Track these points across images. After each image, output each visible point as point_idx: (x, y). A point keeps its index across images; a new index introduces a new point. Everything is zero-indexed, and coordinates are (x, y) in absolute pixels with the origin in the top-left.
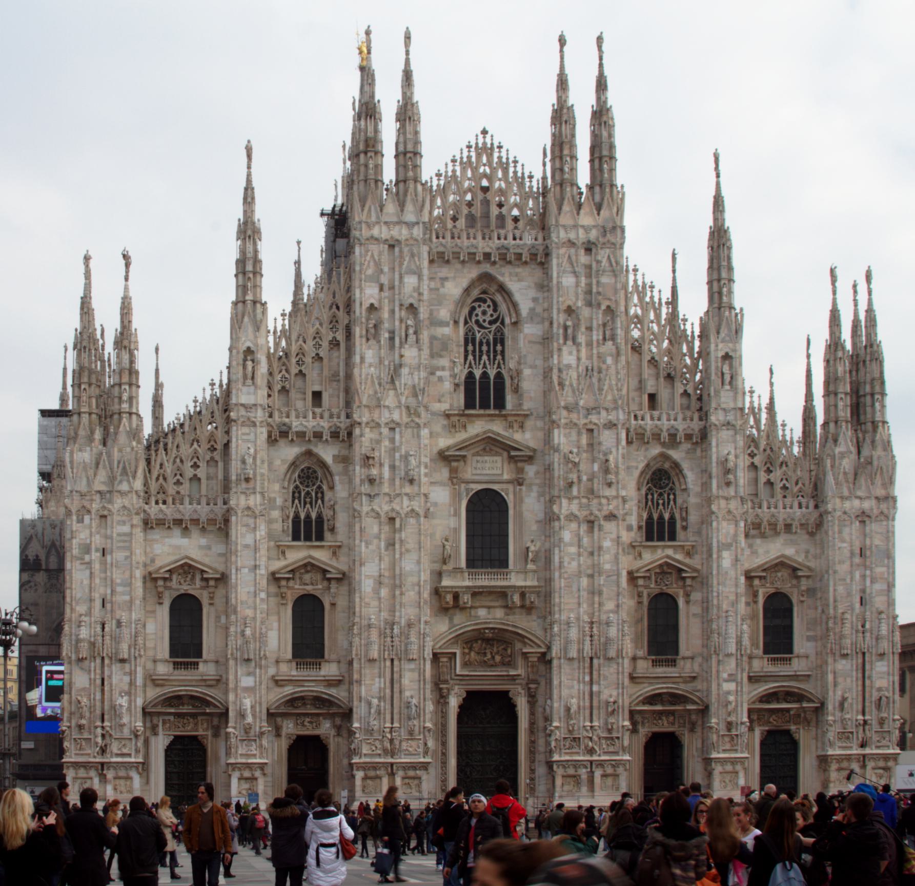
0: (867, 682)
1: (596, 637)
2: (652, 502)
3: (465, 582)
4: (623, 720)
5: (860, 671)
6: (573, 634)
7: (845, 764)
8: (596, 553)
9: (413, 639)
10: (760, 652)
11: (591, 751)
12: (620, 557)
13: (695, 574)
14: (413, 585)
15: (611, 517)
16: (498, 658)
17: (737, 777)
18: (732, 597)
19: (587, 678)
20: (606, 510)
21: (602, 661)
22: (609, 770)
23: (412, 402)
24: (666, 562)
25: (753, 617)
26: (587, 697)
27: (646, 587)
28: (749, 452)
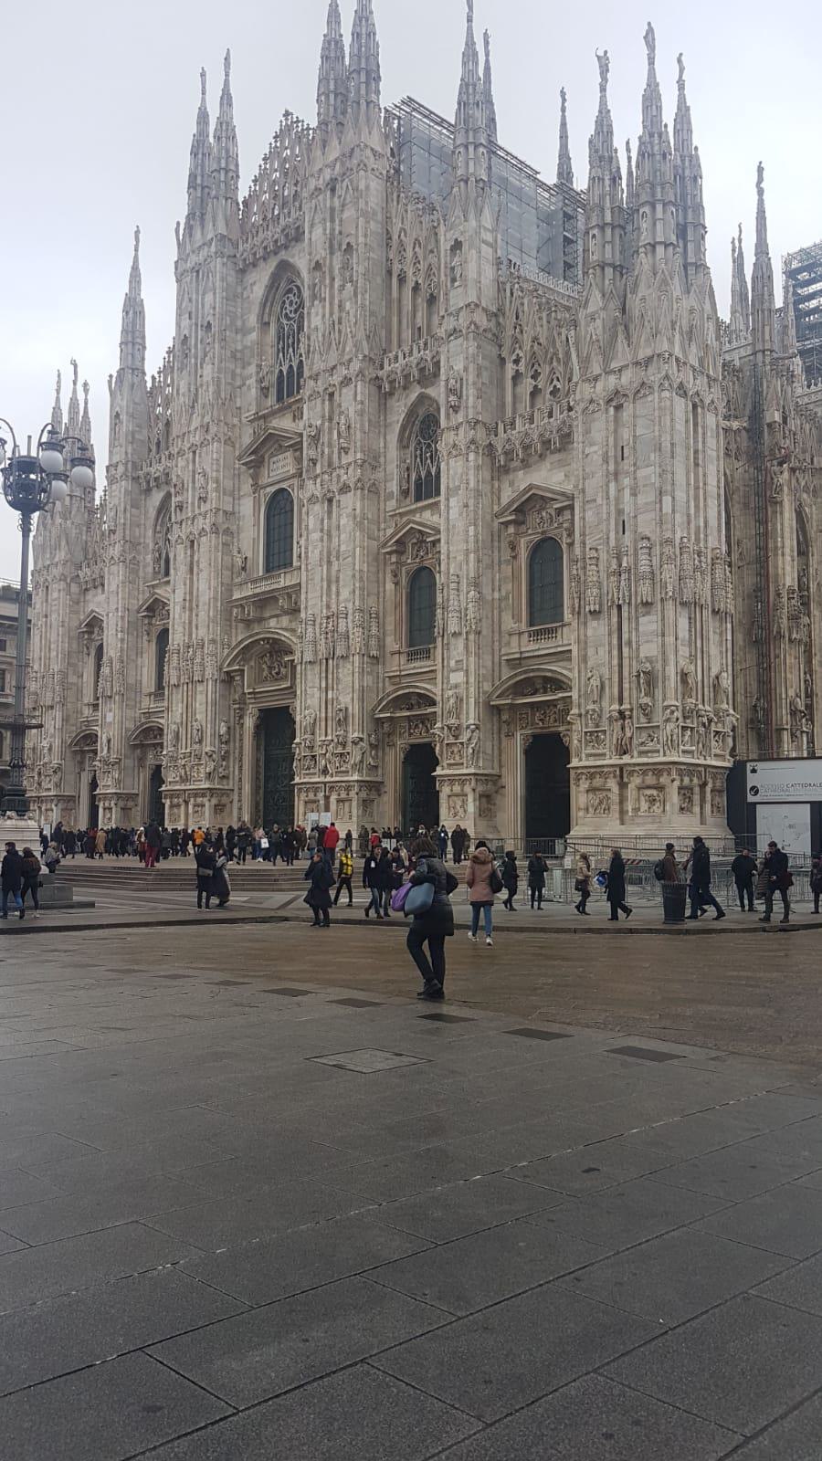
0: (625, 650)
3: (248, 591)
4: (354, 732)
5: (615, 636)
7: (598, 782)
9: (198, 660)
10: (524, 627)
11: (325, 772)
15: (345, 489)
17: (464, 803)
18: (461, 558)
19: (323, 685)
22: (343, 795)
23: (207, 419)
25: (515, 577)
28: (514, 357)
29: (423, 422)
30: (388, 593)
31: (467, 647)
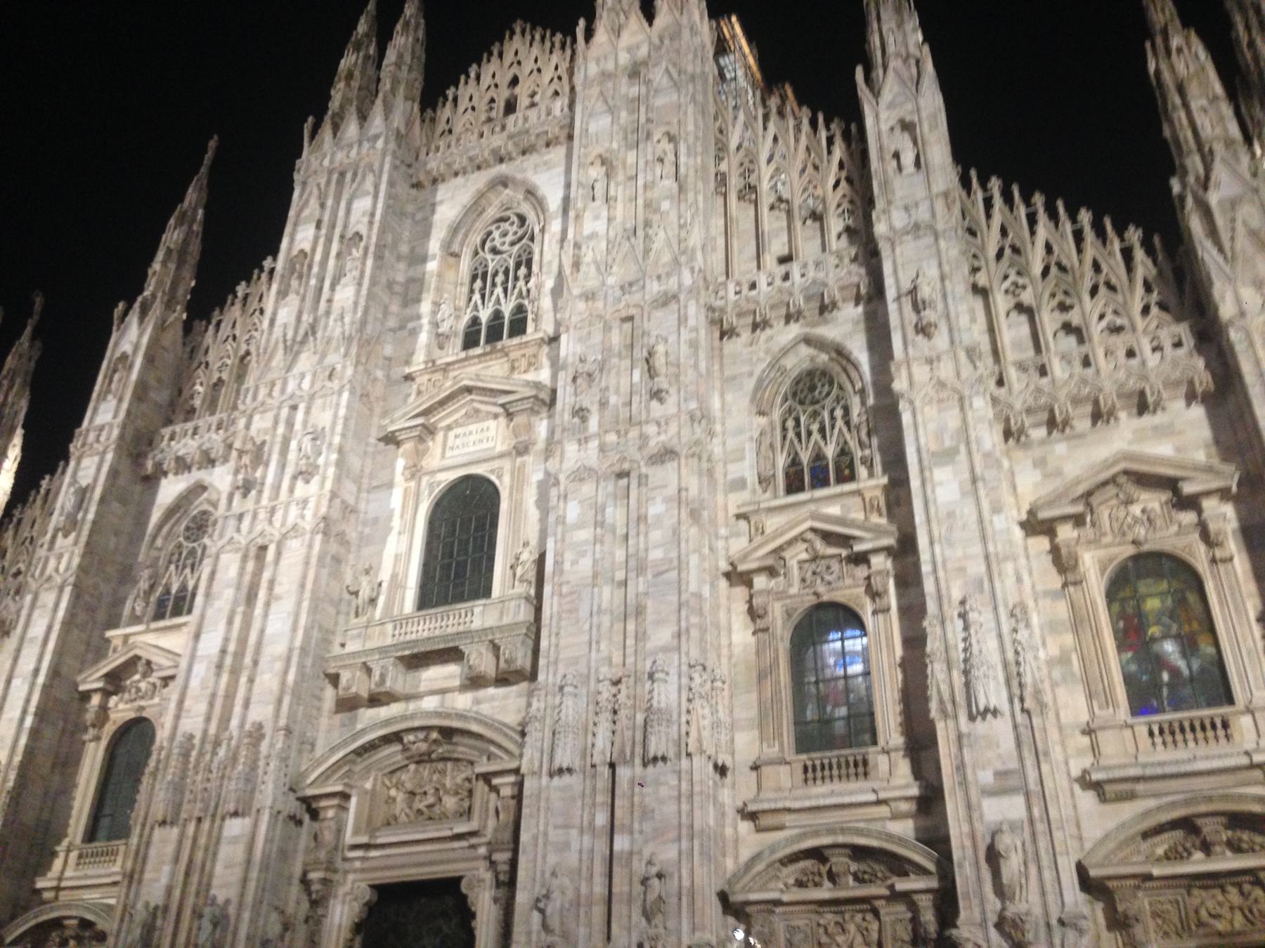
1: (623, 713)
2: (798, 435)
6: (572, 709)
8: (632, 533)
10: (1123, 712)
12: (683, 528)
13: (890, 541)
14: (274, 659)
15: (666, 454)
16: (450, 802)
18: (978, 568)
19: (601, 819)
20: (656, 442)
21: (638, 769)
24: (813, 530)
25: (1077, 623)
26: (599, 868)
27: (781, 595)
28: (1007, 284)
29: (797, 381)
30: (737, 650)
31: (1028, 742)
